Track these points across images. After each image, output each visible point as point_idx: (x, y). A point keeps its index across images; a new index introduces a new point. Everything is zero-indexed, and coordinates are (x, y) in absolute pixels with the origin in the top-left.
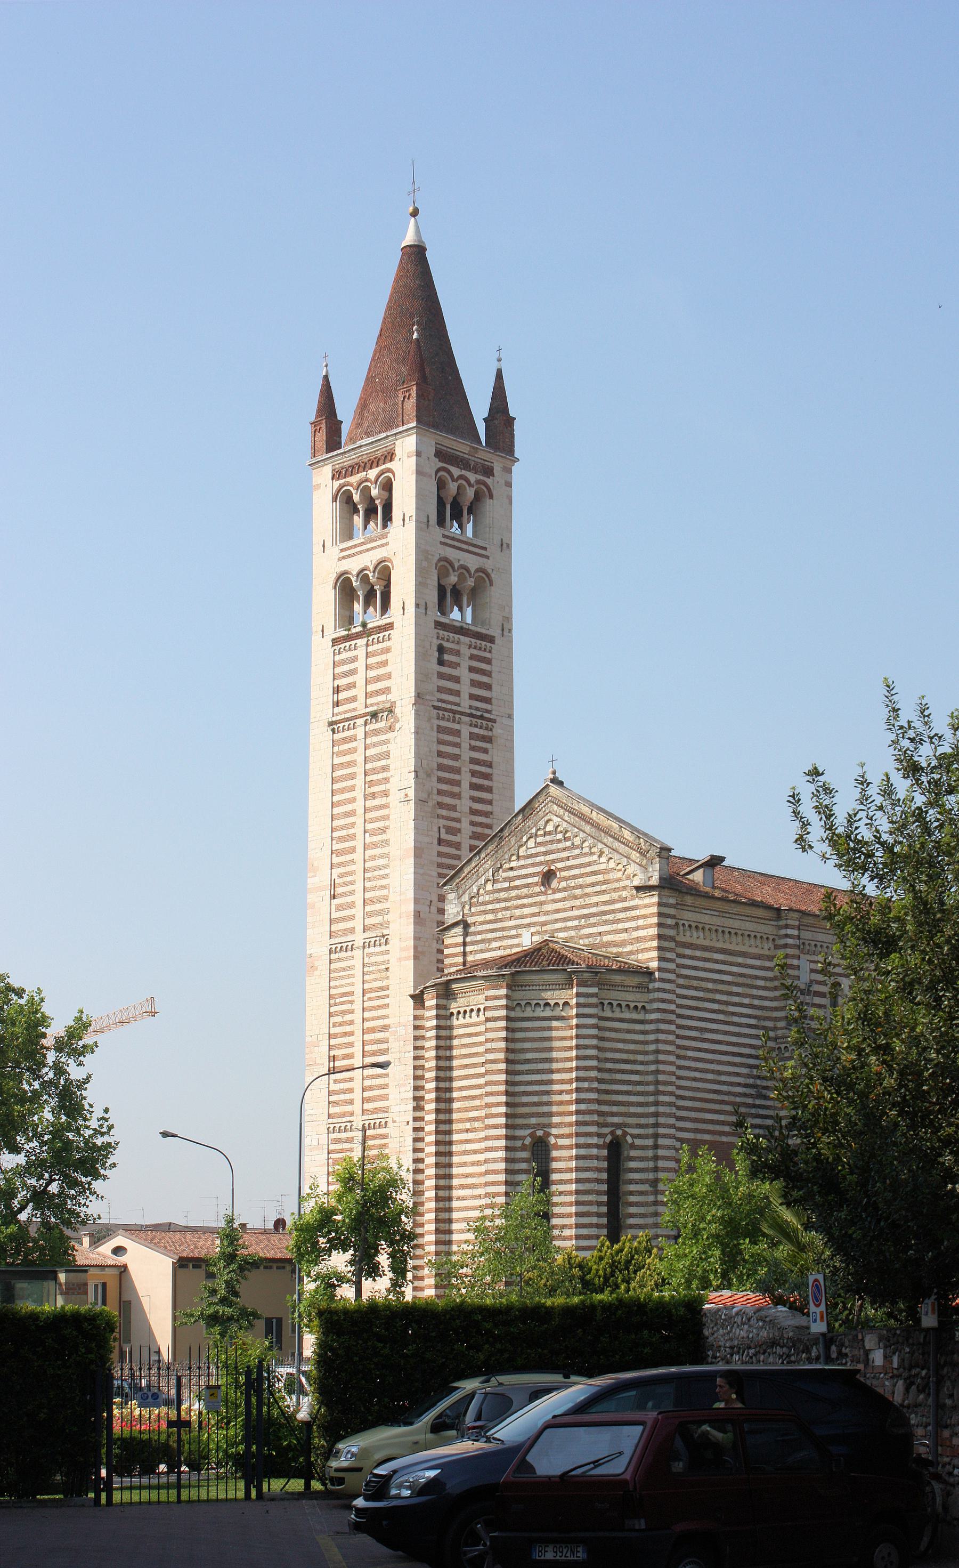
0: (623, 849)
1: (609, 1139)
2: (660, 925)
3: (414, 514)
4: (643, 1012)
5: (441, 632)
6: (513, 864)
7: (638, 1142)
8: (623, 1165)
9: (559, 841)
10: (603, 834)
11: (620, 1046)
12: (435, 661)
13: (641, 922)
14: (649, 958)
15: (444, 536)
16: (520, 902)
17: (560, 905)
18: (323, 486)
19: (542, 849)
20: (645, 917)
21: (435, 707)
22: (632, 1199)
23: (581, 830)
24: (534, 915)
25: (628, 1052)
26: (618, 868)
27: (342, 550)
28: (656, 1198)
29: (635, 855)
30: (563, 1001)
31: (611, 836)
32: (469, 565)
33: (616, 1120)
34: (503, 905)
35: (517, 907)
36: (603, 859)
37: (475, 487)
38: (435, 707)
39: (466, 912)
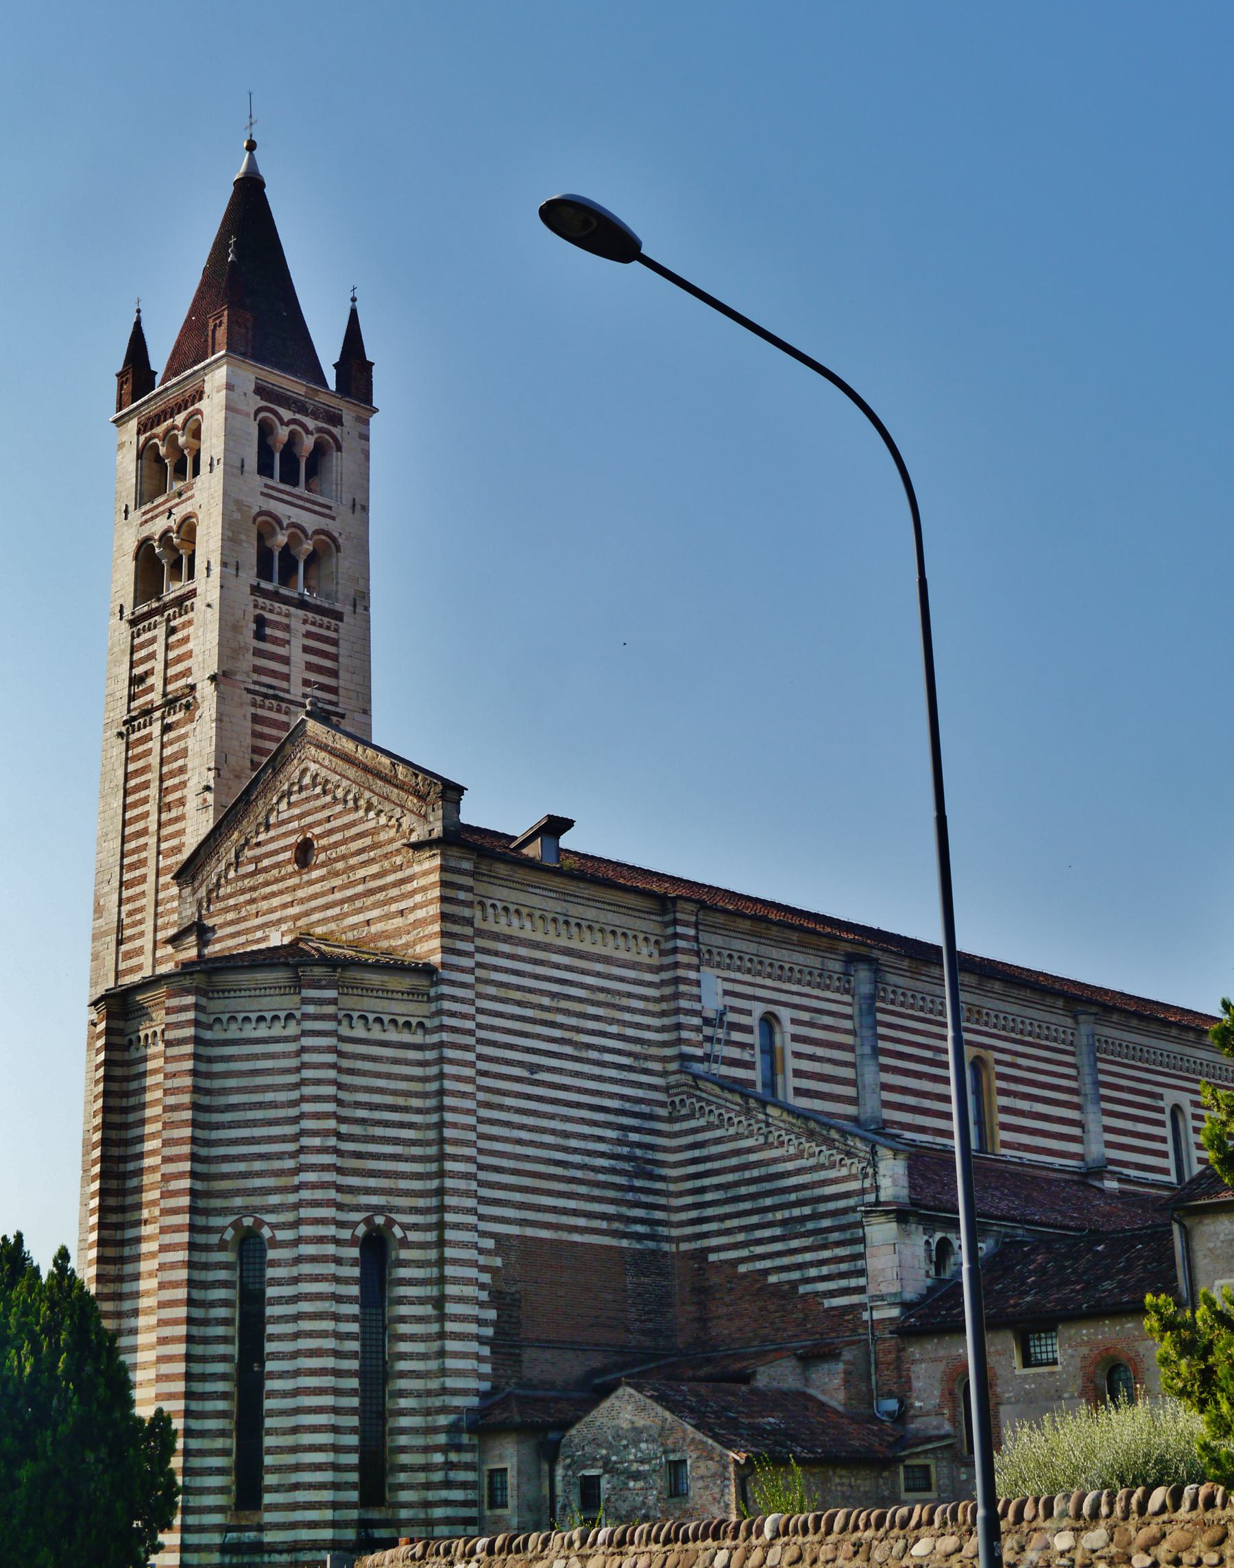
0: (394, 793)
1: (361, 1230)
2: (443, 899)
3: (222, 456)
4: (420, 1032)
5: (261, 600)
6: (262, 837)
7: (413, 1236)
8: (390, 1274)
9: (317, 796)
10: (370, 777)
11: (381, 1083)
12: (251, 634)
13: (418, 898)
14: (429, 949)
15: (266, 486)
16: (268, 890)
17: (317, 888)
18: (127, 444)
19: (296, 811)
20: (424, 889)
21: (249, 691)
22: (403, 1328)
23: (343, 776)
24: (285, 906)
25: (394, 1093)
26: (390, 824)
27: (144, 513)
28: (442, 1326)
29: (412, 801)
30: (286, 1013)
31: (381, 778)
32: (304, 524)
33: (374, 1200)
34: (247, 897)
35: (265, 898)
36: (372, 814)
37: (316, 435)
38: (249, 691)
39: (204, 912)
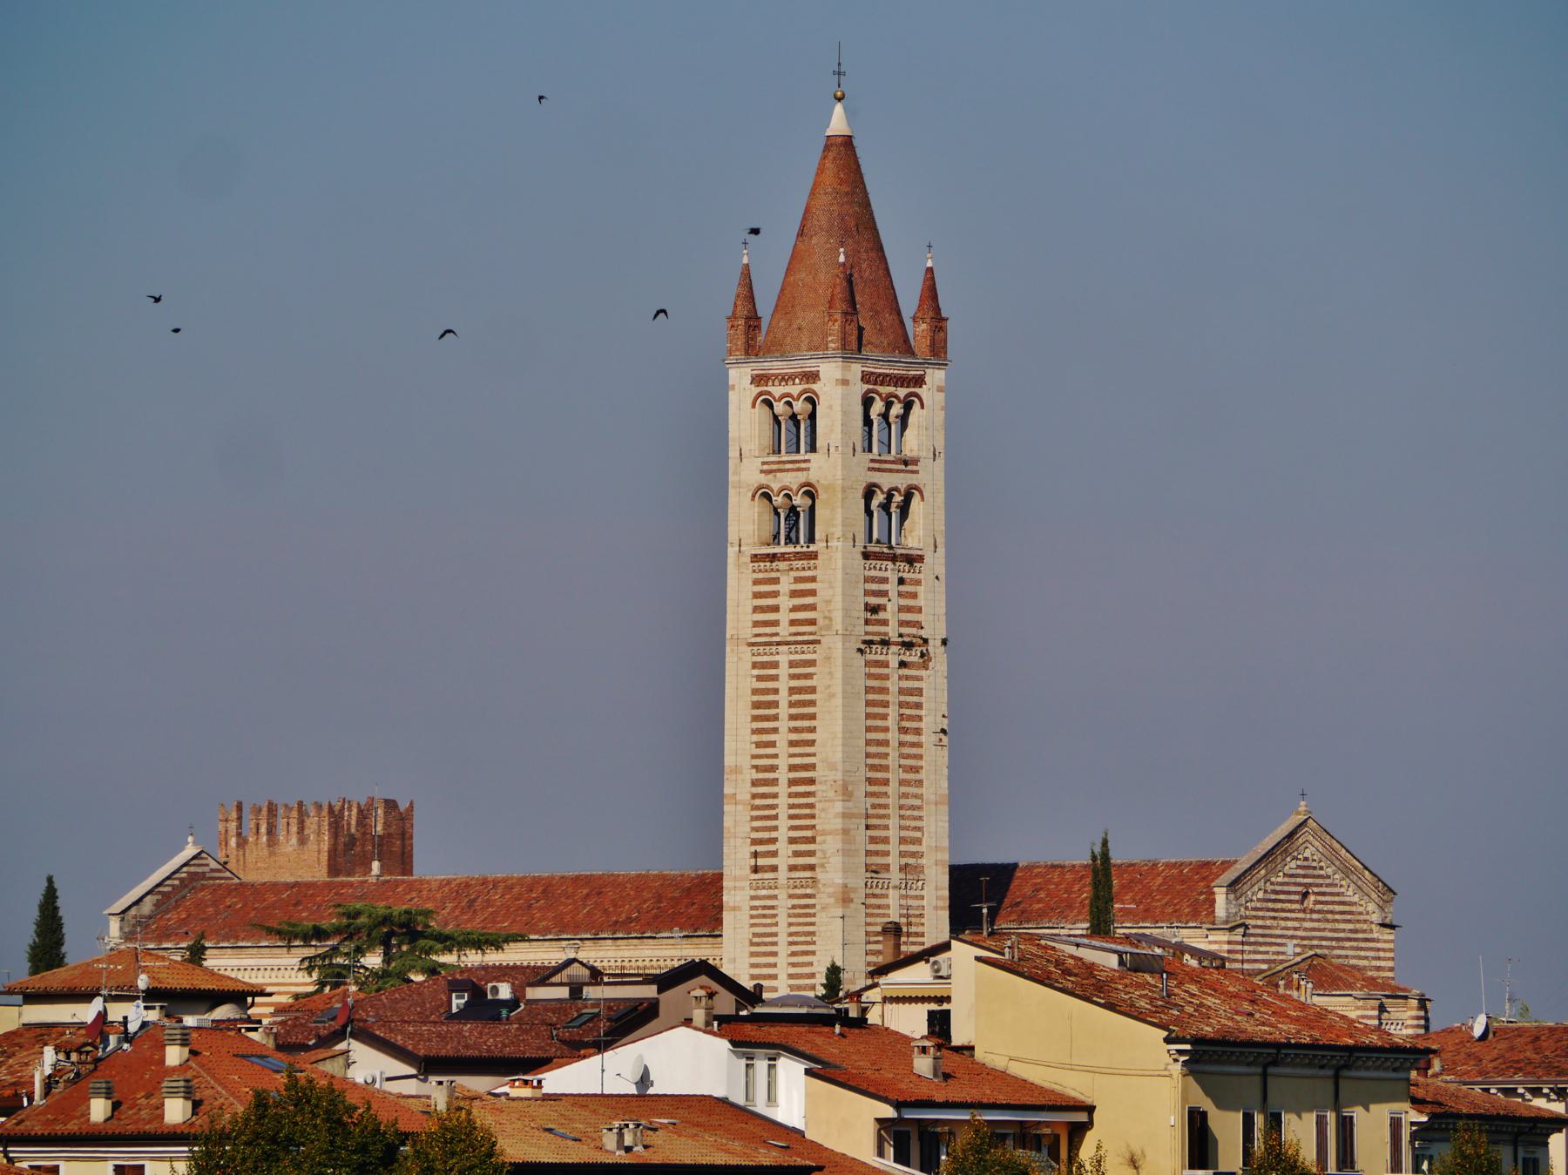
17: (1316, 925)
24: (1295, 929)
35: (1283, 919)
